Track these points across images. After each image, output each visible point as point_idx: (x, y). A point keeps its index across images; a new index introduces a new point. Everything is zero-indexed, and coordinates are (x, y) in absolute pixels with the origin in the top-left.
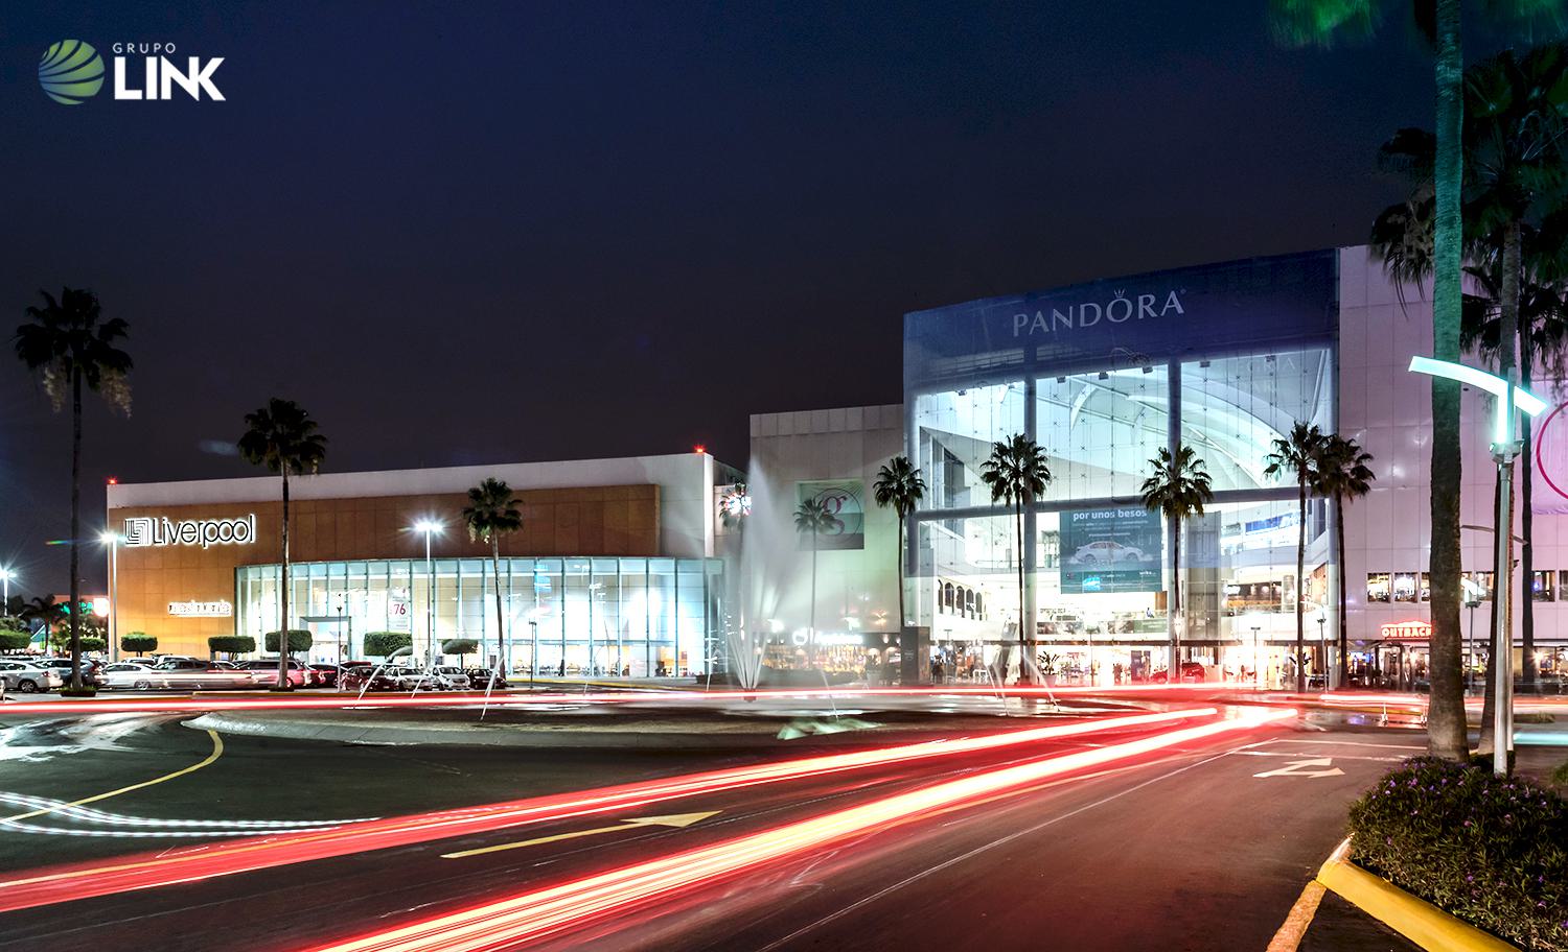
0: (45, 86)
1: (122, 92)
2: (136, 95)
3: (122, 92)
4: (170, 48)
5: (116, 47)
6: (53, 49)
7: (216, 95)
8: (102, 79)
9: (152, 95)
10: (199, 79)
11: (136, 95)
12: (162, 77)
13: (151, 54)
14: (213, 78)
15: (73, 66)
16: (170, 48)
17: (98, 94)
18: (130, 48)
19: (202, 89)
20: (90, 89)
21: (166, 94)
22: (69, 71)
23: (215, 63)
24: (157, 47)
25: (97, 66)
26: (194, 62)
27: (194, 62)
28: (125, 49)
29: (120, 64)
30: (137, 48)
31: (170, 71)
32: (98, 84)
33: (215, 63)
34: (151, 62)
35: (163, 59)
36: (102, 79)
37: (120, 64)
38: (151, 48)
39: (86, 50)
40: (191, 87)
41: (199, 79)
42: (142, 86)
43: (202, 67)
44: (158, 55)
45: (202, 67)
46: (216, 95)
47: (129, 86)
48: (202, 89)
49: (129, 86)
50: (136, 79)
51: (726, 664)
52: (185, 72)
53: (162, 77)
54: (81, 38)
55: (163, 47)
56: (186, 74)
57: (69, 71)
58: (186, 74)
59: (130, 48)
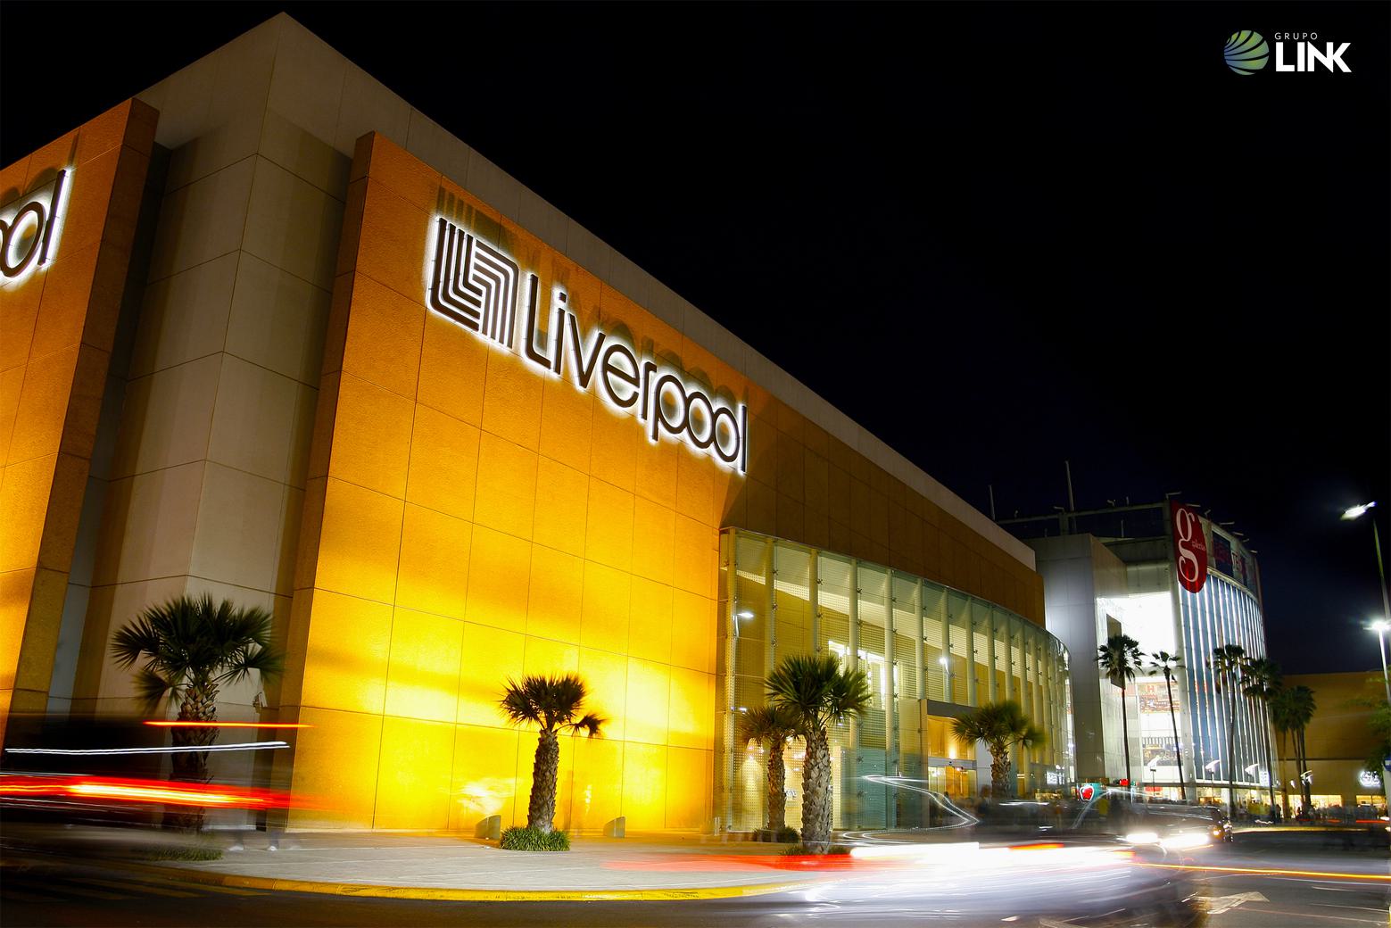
0: (1228, 63)
1: (1281, 67)
2: (1290, 68)
3: (1281, 67)
4: (1314, 36)
5: (1277, 35)
6: (1234, 36)
7: (1345, 68)
8: (1267, 58)
9: (1301, 68)
10: (1334, 57)
11: (1290, 68)
12: (1309, 56)
13: (1301, 40)
14: (1343, 57)
15: (1247, 49)
16: (1314, 36)
17: (1266, 66)
18: (1287, 36)
19: (1335, 65)
20: (1260, 65)
21: (1311, 68)
22: (1245, 52)
23: (1344, 46)
24: (1305, 35)
25: (1264, 48)
26: (1330, 46)
27: (1330, 46)
28: (1283, 36)
29: (1280, 47)
30: (1291, 36)
31: (1314, 52)
32: (1265, 60)
33: (1344, 46)
34: (1301, 46)
35: (1309, 44)
36: (1267, 58)
37: (1280, 47)
38: (1301, 36)
39: (1257, 38)
40: (1328, 63)
41: (1334, 57)
42: (1295, 62)
43: (1335, 49)
44: (1305, 41)
45: (1335, 49)
46: (1345, 68)
47: (1286, 63)
48: (1335, 65)
49: (1286, 63)
50: (1290, 57)
51: (1060, 820)
52: (1324, 53)
53: (1309, 56)
54: (1253, 29)
55: (1309, 36)
56: (1325, 54)
57: (1245, 52)
58: (1325, 54)
59: (1287, 36)
